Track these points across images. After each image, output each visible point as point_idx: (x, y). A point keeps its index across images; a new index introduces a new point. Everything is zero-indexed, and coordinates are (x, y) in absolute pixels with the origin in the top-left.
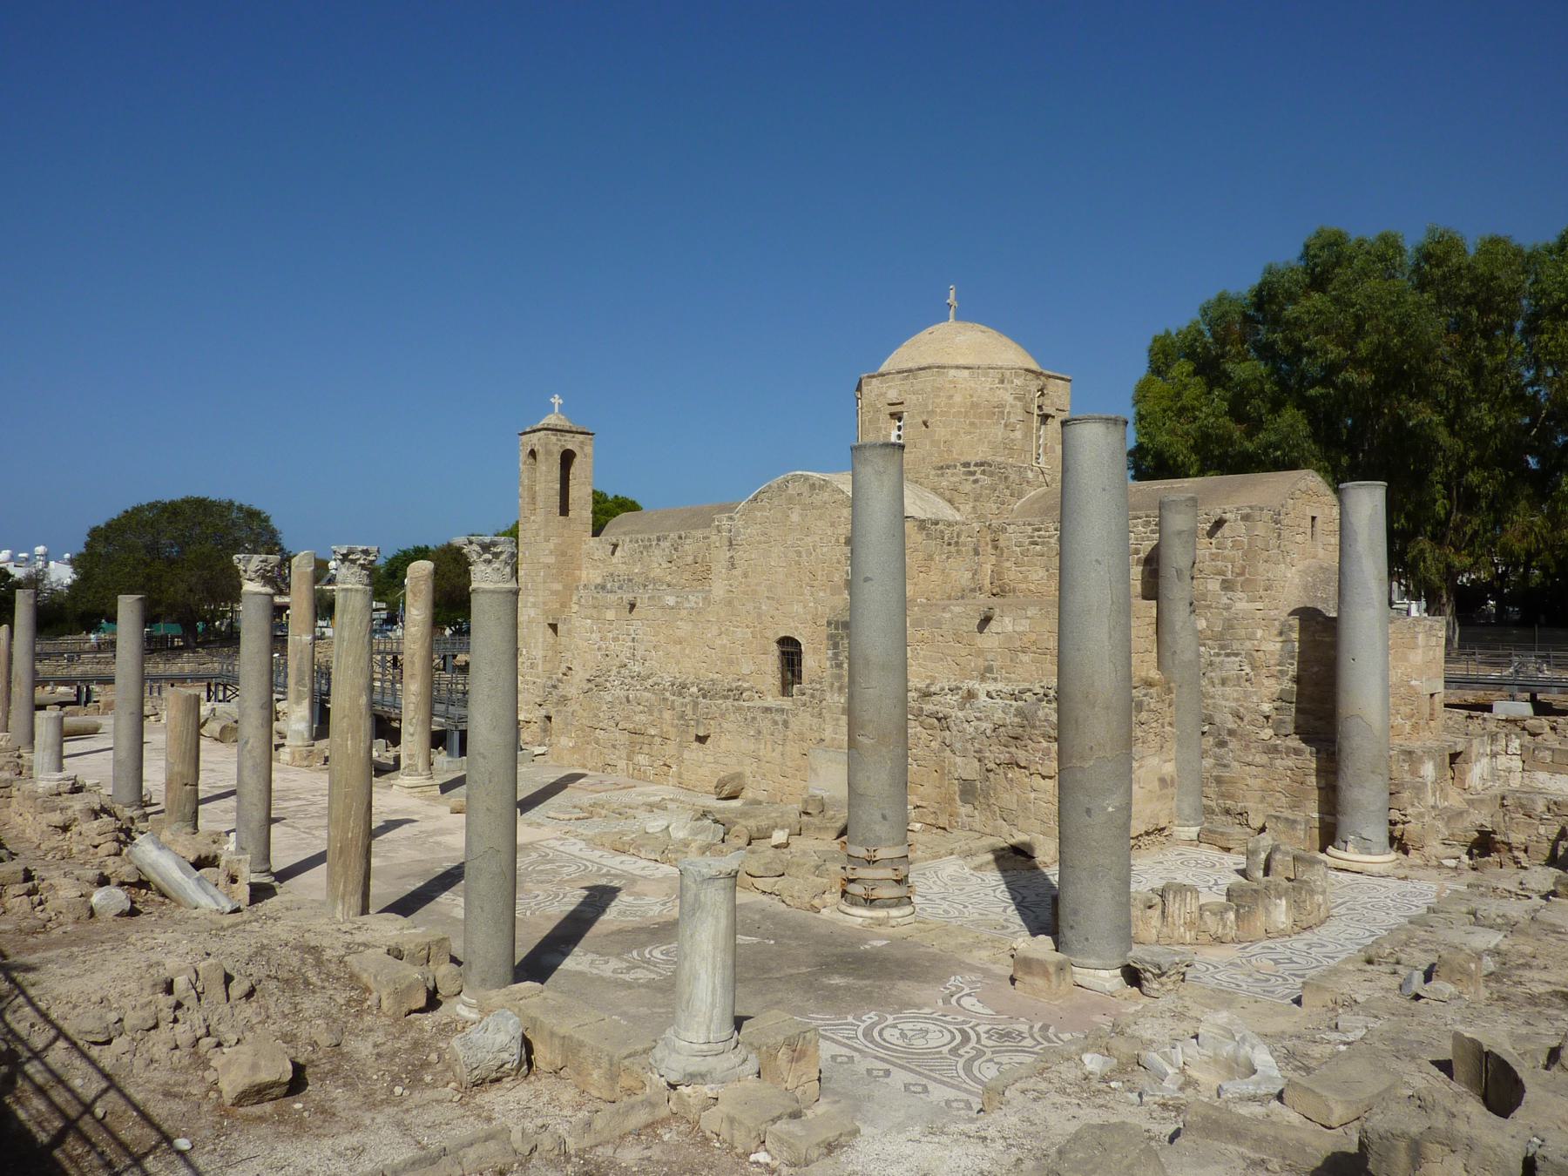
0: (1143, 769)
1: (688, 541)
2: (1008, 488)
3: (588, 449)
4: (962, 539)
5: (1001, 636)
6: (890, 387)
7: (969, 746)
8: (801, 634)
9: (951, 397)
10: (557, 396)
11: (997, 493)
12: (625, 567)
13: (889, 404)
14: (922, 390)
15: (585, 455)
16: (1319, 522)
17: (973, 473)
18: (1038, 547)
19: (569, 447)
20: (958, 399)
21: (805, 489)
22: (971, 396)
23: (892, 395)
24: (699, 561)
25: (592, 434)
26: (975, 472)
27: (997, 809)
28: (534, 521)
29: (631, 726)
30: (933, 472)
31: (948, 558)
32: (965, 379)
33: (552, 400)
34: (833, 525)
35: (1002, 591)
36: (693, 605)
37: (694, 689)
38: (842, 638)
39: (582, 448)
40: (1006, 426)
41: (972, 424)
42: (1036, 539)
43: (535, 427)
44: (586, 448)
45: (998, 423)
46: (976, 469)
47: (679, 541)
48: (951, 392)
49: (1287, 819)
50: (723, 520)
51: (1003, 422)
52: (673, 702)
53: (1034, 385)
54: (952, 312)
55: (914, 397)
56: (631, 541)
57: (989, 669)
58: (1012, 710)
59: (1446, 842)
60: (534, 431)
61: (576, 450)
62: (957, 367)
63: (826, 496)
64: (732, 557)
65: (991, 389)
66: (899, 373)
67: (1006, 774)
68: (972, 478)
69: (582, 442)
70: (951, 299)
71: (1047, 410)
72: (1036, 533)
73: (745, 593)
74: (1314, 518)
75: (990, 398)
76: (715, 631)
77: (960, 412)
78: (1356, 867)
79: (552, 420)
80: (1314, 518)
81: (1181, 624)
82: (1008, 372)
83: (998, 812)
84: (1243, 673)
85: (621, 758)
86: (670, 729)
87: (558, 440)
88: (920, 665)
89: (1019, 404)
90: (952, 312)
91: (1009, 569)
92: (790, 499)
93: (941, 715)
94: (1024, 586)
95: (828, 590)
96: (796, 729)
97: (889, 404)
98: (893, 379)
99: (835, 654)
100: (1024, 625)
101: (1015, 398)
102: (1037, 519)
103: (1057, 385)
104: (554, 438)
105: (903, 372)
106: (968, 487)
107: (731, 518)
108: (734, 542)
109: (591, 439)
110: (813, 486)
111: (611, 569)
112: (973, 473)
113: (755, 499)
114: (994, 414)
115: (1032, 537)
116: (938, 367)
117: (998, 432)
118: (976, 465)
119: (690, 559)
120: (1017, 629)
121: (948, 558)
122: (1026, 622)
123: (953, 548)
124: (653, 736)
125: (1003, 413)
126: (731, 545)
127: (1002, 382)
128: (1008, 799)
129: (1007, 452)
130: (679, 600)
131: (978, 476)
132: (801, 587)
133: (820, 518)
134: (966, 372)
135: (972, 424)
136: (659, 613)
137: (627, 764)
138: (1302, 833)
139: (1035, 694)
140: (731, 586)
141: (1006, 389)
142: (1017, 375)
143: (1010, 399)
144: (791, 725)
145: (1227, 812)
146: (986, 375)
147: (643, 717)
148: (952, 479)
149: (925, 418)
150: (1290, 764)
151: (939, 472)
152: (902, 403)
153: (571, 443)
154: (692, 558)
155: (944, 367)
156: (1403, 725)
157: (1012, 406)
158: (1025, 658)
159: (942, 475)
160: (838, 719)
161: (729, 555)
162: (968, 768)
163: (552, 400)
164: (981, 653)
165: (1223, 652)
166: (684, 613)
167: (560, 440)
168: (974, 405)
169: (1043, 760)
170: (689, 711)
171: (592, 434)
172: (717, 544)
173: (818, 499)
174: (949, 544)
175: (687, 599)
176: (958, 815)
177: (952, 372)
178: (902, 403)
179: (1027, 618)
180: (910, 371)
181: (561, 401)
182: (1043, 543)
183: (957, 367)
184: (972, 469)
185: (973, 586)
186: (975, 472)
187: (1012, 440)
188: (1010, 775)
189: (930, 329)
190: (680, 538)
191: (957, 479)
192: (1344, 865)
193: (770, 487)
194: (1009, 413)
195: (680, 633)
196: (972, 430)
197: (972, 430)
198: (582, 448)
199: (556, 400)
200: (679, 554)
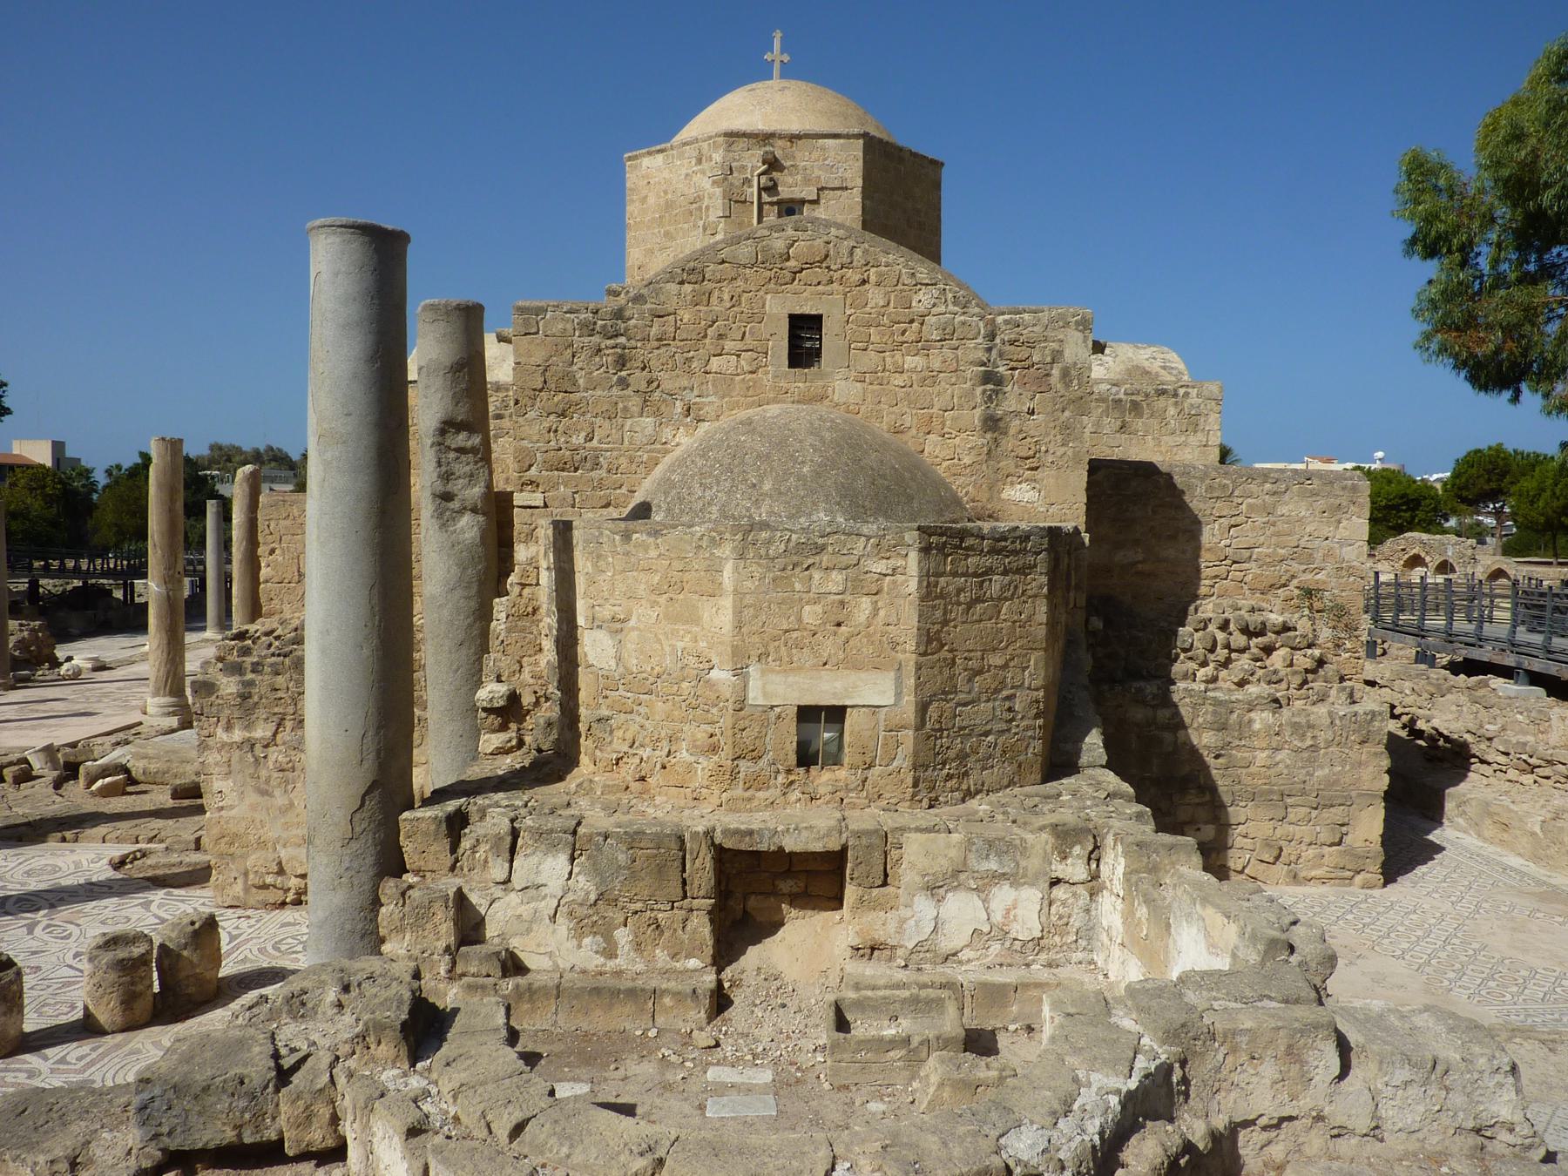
20: (652, 200)
22: (666, 192)
32: (659, 169)
40: (705, 229)
51: (701, 223)
53: (753, 161)
71: (785, 192)
82: (705, 145)
101: (714, 182)
103: (823, 149)
125: (700, 208)
127: (699, 161)
135: (667, 234)
141: (703, 172)
142: (716, 146)
143: (706, 184)
146: (681, 156)
156: (690, 768)
194: (707, 208)
196: (669, 244)
197: (669, 244)
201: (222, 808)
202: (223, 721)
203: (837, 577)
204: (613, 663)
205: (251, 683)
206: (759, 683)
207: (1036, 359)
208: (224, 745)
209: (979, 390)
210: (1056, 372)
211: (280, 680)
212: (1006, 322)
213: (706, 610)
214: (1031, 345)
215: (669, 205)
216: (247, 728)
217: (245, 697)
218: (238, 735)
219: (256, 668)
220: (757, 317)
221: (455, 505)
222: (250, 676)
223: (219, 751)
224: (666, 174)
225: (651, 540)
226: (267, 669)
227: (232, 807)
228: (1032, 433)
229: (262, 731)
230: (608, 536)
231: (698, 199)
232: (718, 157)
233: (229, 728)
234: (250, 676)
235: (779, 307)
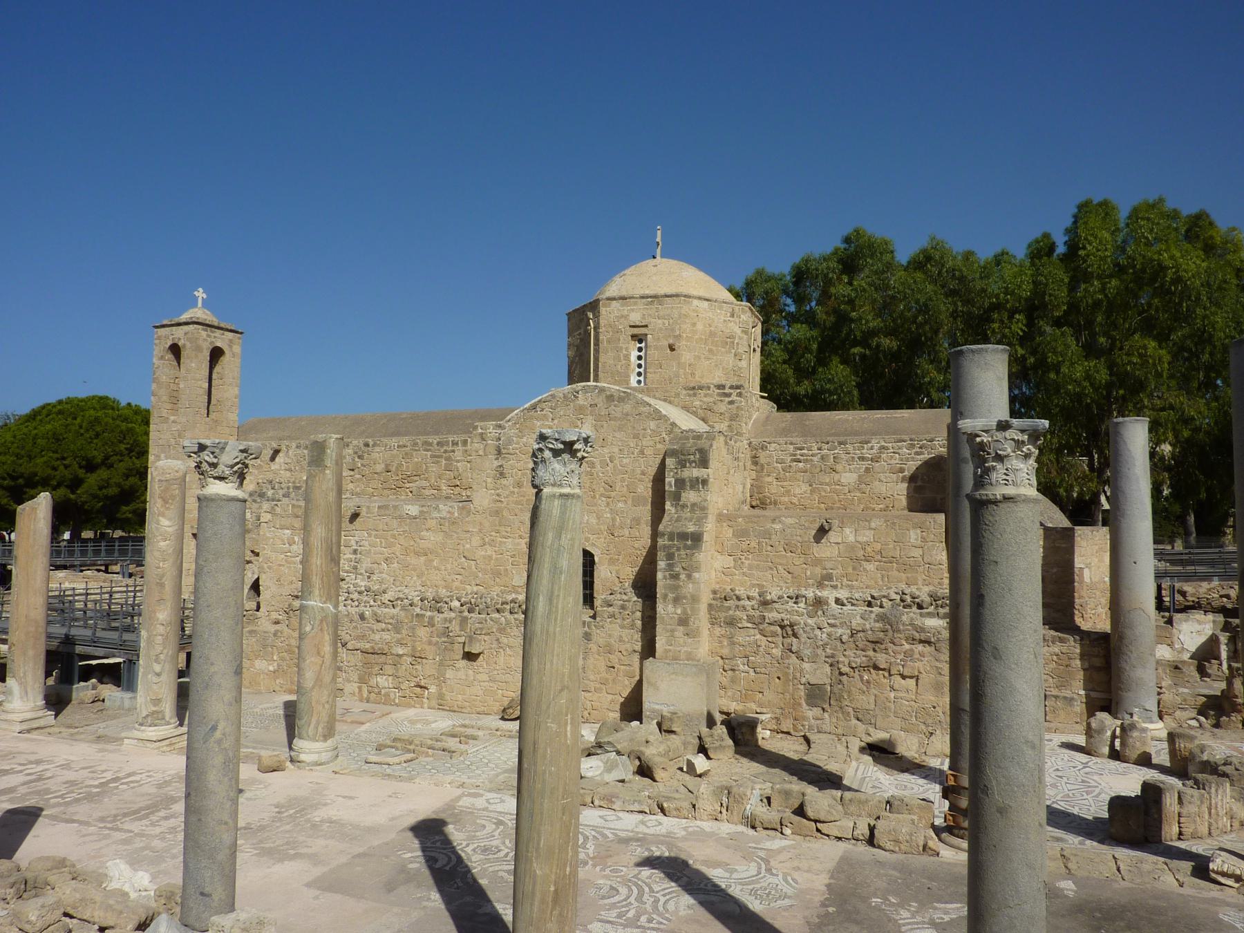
1: (377, 449)
3: (237, 349)
5: (841, 546)
6: (633, 310)
7: (820, 651)
8: (593, 545)
9: (694, 324)
10: (201, 290)
12: (288, 474)
13: (630, 326)
14: (669, 315)
15: (234, 355)
17: (729, 395)
18: (801, 465)
19: (219, 344)
20: (700, 327)
21: (600, 401)
22: (710, 326)
23: (635, 318)
24: (393, 469)
25: (241, 333)
26: (731, 394)
27: (850, 710)
28: (173, 422)
29: (368, 646)
30: (684, 392)
32: (705, 310)
33: (196, 293)
34: (636, 436)
35: (762, 503)
36: (444, 514)
37: (456, 604)
38: (678, 549)
39: (230, 347)
40: (735, 355)
41: (710, 351)
42: (799, 457)
43: (176, 320)
44: (235, 347)
46: (732, 391)
47: (366, 449)
48: (695, 320)
49: (1065, 698)
50: (490, 428)
51: (733, 351)
52: (431, 618)
54: (659, 251)
56: (297, 447)
57: (829, 577)
58: (873, 616)
60: (179, 324)
61: (225, 348)
62: (700, 298)
63: (627, 407)
64: (501, 466)
65: (725, 321)
66: (642, 297)
67: (861, 677)
68: (727, 399)
69: (231, 341)
70: (659, 239)
72: (799, 452)
73: (517, 503)
75: (724, 329)
76: (476, 541)
77: (701, 339)
79: (199, 313)
83: (852, 713)
85: (349, 681)
86: (427, 647)
87: (209, 336)
88: (744, 574)
89: (745, 337)
90: (659, 251)
91: (770, 484)
92: (581, 409)
93: (786, 622)
94: (786, 499)
95: (630, 502)
96: (601, 642)
97: (630, 326)
98: (635, 304)
99: (669, 565)
100: (866, 536)
101: (743, 331)
102: (798, 439)
104: (204, 334)
105: (647, 297)
106: (723, 407)
107: (500, 426)
108: (504, 451)
109: (239, 338)
110: (610, 398)
111: (270, 476)
112: (729, 395)
113: (534, 407)
114: (727, 343)
115: (795, 455)
116: (685, 296)
117: (730, 360)
118: (731, 387)
119: (380, 468)
122: (870, 534)
124: (400, 656)
126: (499, 452)
127: (732, 316)
128: (865, 701)
130: (425, 509)
131: (734, 397)
132: (594, 497)
133: (620, 429)
134: (706, 303)
135: (710, 351)
136: (395, 523)
137: (360, 688)
139: (891, 600)
140: (498, 495)
141: (735, 323)
144: (594, 638)
146: (721, 308)
147: (387, 636)
148: (705, 399)
149: (671, 341)
150: (1057, 650)
151: (692, 392)
152: (646, 326)
153: (221, 340)
154: (383, 466)
155: (689, 297)
157: (740, 338)
158: (870, 567)
159: (695, 395)
160: (672, 631)
161: (496, 463)
162: (820, 674)
163: (196, 293)
164: (818, 562)
166: (432, 523)
167: (209, 336)
168: (712, 334)
169: (906, 661)
170: (455, 627)
171: (241, 333)
172: (481, 453)
173: (617, 410)
175: (437, 508)
176: (804, 718)
177: (696, 302)
178: (646, 326)
179: (870, 529)
180: (655, 297)
181: (205, 296)
182: (806, 461)
183: (700, 298)
184: (727, 391)
186: (731, 394)
187: (740, 368)
188: (866, 677)
189: (647, 261)
190: (367, 445)
191: (712, 400)
193: (553, 396)
195: (424, 545)
198: (230, 347)
199: (200, 294)
200: (364, 462)
224: (710, 314)
231: (732, 337)
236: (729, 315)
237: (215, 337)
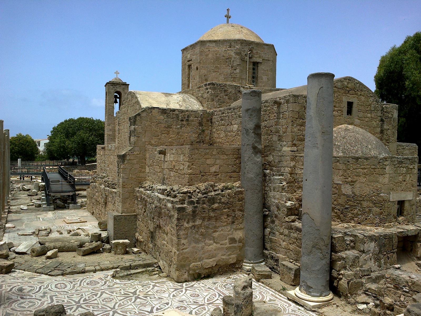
0: (217, 233)
2: (226, 95)
4: (191, 118)
6: (188, 53)
9: (207, 55)
11: (219, 97)
13: (189, 61)
16: (355, 106)
19: (118, 90)
20: (210, 56)
22: (216, 54)
31: (181, 127)
40: (232, 67)
45: (228, 65)
51: (231, 65)
55: (194, 56)
59: (367, 292)
65: (225, 50)
69: (124, 88)
74: (350, 105)
75: (225, 55)
78: (302, 302)
80: (350, 105)
81: (247, 158)
84: (282, 185)
89: (238, 57)
104: (112, 87)
112: (207, 89)
115: (221, 117)
120: (171, 159)
121: (181, 127)
123: (184, 123)
125: (230, 61)
129: (232, 79)
134: (214, 44)
138: (293, 275)
141: (231, 50)
143: (232, 54)
145: (272, 257)
152: (191, 60)
157: (235, 58)
158: (172, 174)
165: (278, 174)
167: (114, 88)
174: (182, 121)
177: (208, 44)
178: (191, 60)
185: (198, 140)
192: (297, 300)
201: (183, 249)
202: (187, 220)
203: (405, 169)
204: (351, 193)
205: (196, 207)
206: (392, 196)
207: (389, 116)
208: (186, 228)
209: (380, 123)
210: (392, 119)
211: (205, 205)
212: (385, 107)
213: (381, 179)
214: (388, 113)
215: (217, 59)
216: (194, 222)
217: (194, 212)
218: (191, 224)
219: (198, 202)
220: (341, 101)
221: (257, 150)
222: (196, 205)
223: (184, 230)
224: (217, 49)
225: (365, 160)
226: (201, 202)
227: (186, 248)
228: (388, 134)
229: (198, 222)
230: (351, 160)
231: (229, 58)
232: (238, 47)
233: (188, 223)
234: (196, 205)
235: (345, 99)
236: (228, 47)
237: (116, 88)
